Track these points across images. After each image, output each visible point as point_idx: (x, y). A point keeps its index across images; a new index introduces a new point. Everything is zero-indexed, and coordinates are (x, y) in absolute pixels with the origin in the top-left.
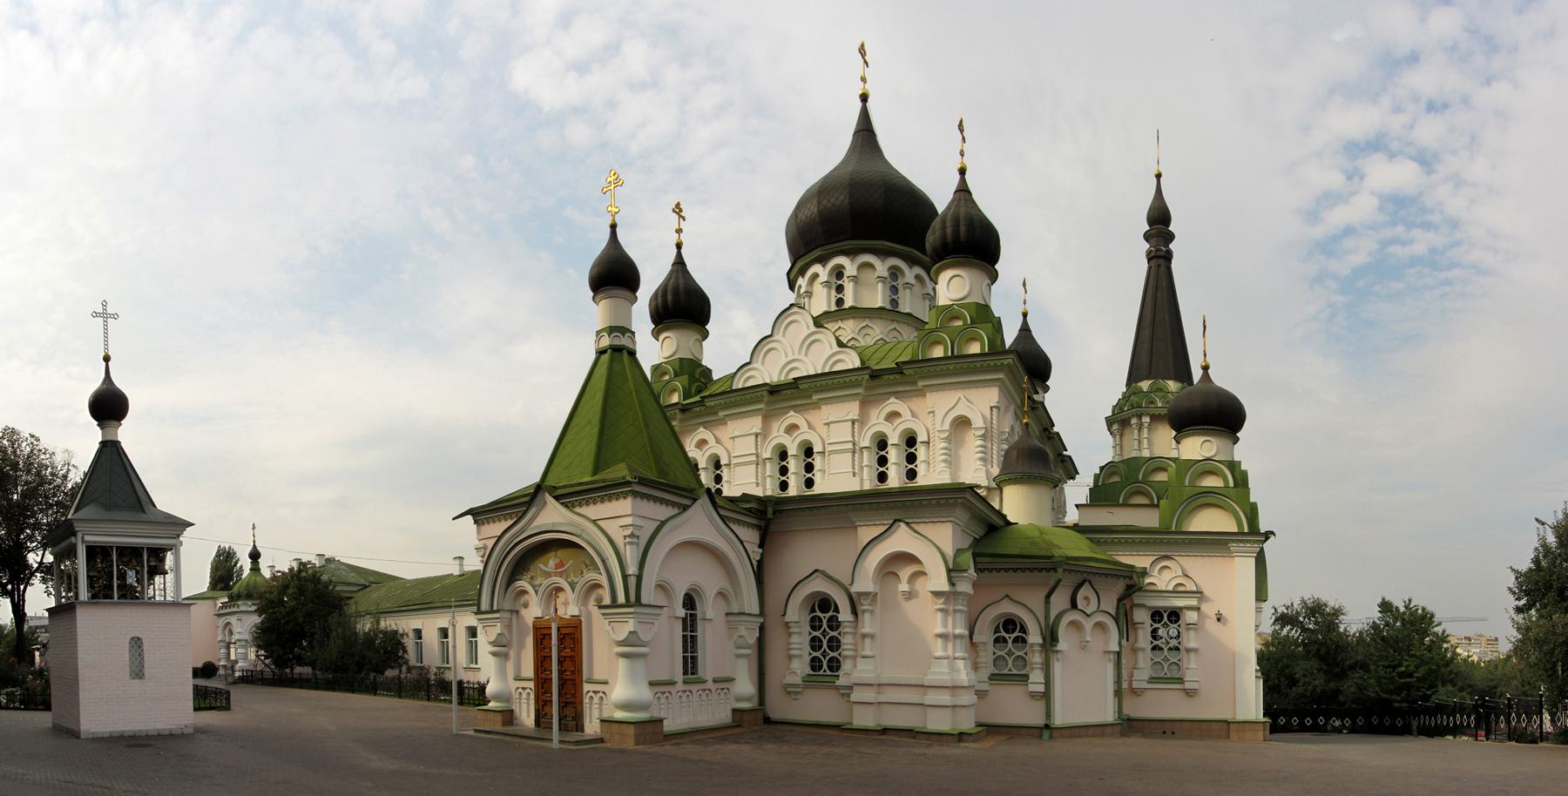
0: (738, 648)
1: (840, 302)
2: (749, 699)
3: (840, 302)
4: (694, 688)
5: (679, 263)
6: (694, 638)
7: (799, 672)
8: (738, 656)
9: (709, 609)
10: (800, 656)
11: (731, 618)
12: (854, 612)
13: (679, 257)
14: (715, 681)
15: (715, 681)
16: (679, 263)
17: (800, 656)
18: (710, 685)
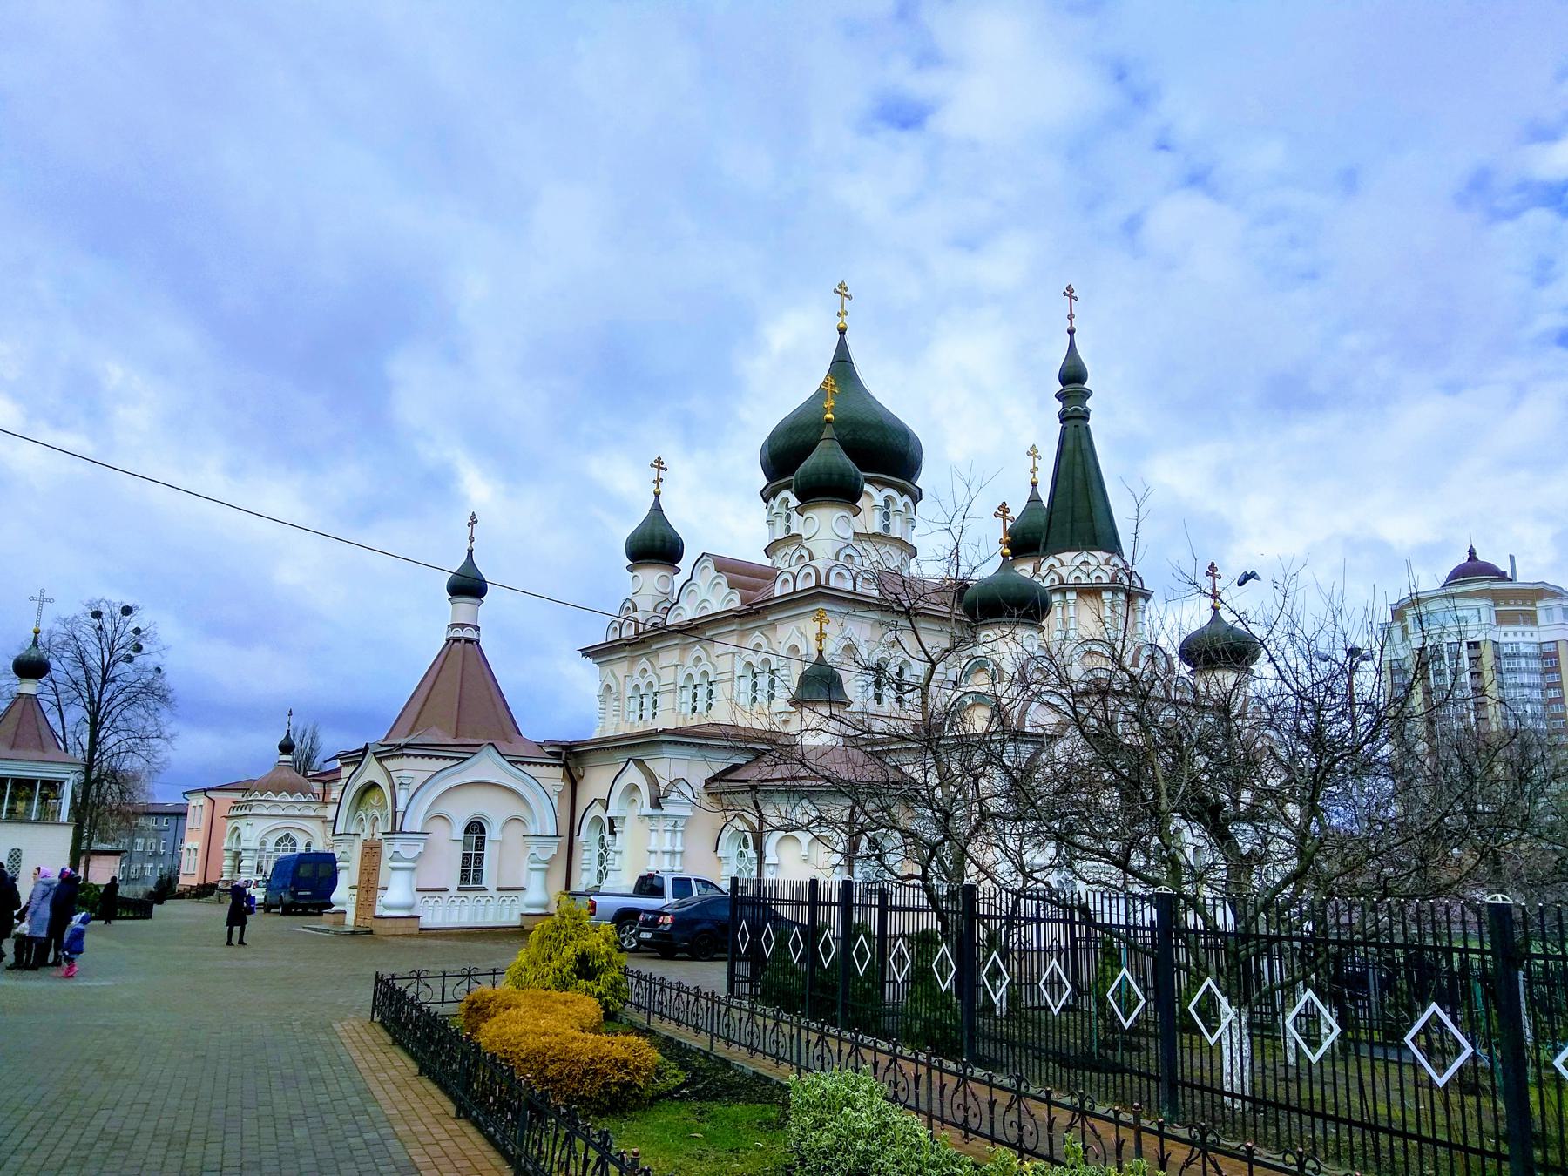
0: (532, 862)
1: (788, 529)
2: (545, 906)
3: (788, 529)
4: (471, 895)
5: (657, 509)
6: (480, 859)
7: (585, 883)
8: (531, 869)
9: (492, 833)
10: (588, 870)
11: (526, 839)
12: (613, 833)
13: (657, 502)
14: (499, 889)
15: (499, 889)
16: (657, 509)
17: (588, 870)
18: (492, 891)
